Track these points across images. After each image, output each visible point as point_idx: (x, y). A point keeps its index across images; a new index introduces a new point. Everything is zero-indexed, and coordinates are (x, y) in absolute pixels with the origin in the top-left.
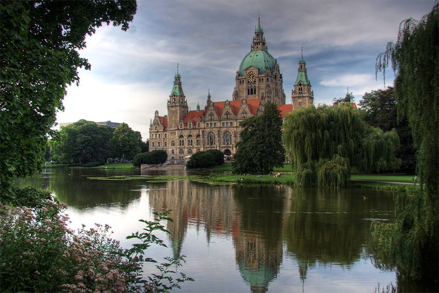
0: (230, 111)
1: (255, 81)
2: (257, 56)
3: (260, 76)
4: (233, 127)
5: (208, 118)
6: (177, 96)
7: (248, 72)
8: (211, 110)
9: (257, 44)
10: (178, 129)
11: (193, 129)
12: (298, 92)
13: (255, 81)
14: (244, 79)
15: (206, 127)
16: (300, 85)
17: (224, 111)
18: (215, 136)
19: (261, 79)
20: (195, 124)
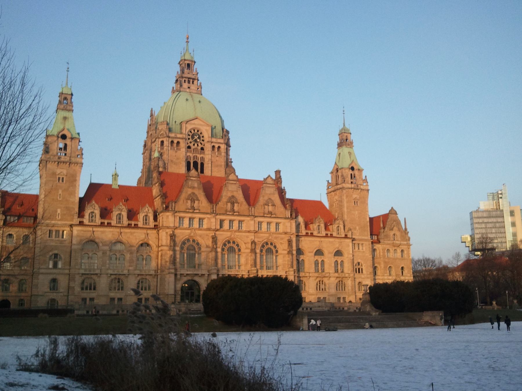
0: (240, 196)
1: (202, 149)
2: (200, 102)
3: (214, 140)
4: (249, 232)
5: (183, 204)
6: (72, 139)
7: (189, 127)
8: (194, 188)
9: (189, 82)
10: (81, 223)
11: (129, 226)
12: (350, 181)
13: (202, 149)
14: (182, 139)
15: (177, 225)
16: (353, 169)
17: (226, 195)
18: (200, 248)
19: (217, 146)
20: (132, 215)
